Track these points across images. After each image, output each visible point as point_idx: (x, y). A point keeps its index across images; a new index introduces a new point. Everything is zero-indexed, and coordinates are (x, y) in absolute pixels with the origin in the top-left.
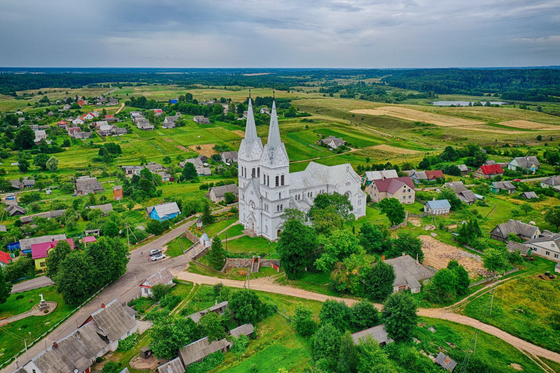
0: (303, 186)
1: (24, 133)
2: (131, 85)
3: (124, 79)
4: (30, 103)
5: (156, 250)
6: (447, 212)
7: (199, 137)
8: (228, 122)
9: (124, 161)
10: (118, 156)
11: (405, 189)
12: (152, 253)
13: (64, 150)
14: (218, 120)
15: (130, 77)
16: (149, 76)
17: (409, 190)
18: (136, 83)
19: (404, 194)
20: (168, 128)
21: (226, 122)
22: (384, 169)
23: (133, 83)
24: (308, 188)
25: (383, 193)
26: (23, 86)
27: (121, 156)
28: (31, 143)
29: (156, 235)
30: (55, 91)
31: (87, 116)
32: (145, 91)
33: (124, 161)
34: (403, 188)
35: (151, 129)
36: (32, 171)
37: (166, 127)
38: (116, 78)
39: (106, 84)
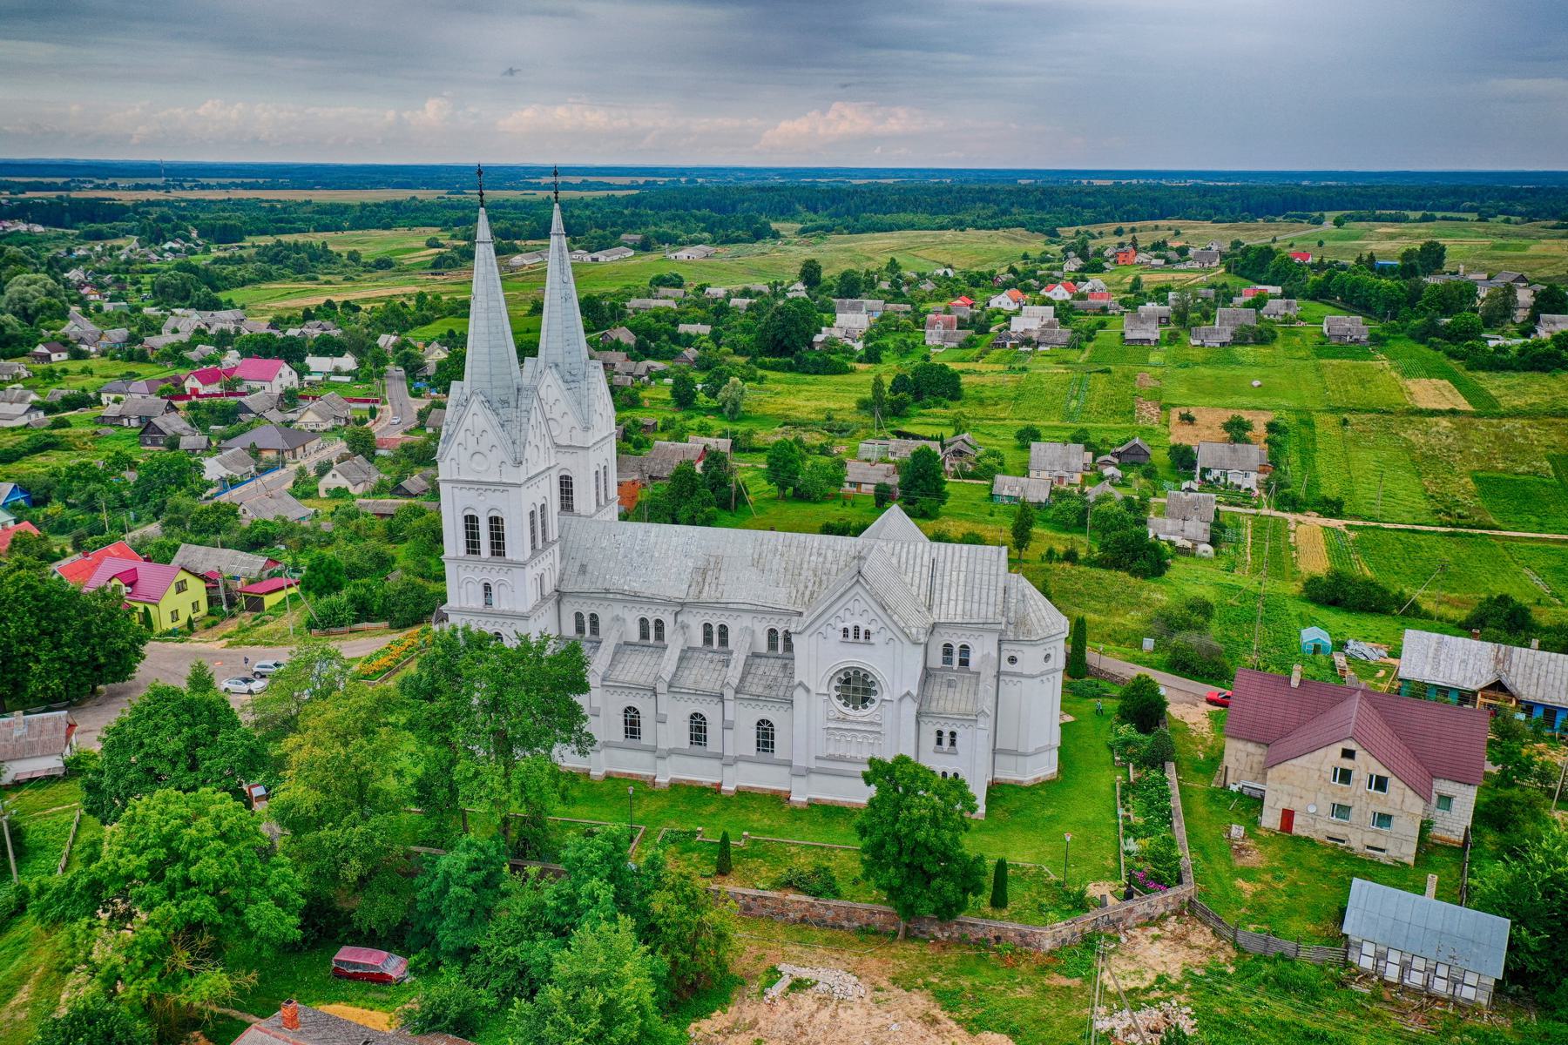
0: (679, 591)
1: (781, 314)
2: (1406, 219)
3: (1414, 202)
4: (1029, 253)
5: (271, 664)
6: (1468, 993)
7: (1256, 383)
8: (1437, 349)
9: (937, 421)
10: (938, 404)
11: (1347, 764)
12: (255, 669)
13: (853, 371)
14: (1412, 337)
15: (1421, 197)
16: (1446, 193)
17: (1381, 784)
18: (1419, 214)
19: (1343, 794)
20: (1203, 346)
21: (1433, 346)
22: (1535, 643)
23: (1412, 215)
24: (698, 605)
25: (1251, 747)
26: (1107, 214)
27: (946, 407)
28: (786, 342)
29: (391, 627)
30: (1157, 227)
31: (1055, 290)
32: (1401, 235)
33: (937, 421)
34: (1331, 756)
35: (1149, 341)
36: (699, 408)
37: (1198, 342)
38: (1390, 197)
39: (1316, 214)
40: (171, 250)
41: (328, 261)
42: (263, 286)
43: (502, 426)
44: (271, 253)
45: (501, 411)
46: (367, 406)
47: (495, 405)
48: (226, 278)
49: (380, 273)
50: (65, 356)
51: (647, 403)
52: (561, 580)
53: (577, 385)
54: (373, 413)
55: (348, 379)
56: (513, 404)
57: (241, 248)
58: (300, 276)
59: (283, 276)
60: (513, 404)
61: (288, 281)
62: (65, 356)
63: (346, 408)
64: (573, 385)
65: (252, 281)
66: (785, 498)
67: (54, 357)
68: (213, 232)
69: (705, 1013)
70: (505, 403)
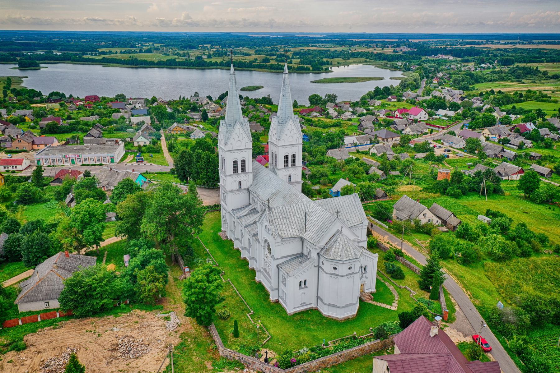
40: (481, 67)
41: (534, 75)
42: (497, 83)
43: (227, 132)
44: (512, 70)
45: (229, 128)
46: (431, 128)
47: (228, 125)
48: (484, 79)
49: (552, 80)
50: (396, 100)
51: (555, 148)
52: (251, 185)
53: (282, 125)
54: (431, 132)
55: (446, 119)
56: (232, 126)
57: (508, 67)
58: (514, 80)
59: (509, 79)
60: (232, 126)
61: (509, 81)
62: (396, 100)
63: (426, 128)
64: (281, 125)
65: (495, 80)
66: (525, 198)
67: (392, 100)
68: (502, 61)
69: (141, 310)
70: (230, 125)
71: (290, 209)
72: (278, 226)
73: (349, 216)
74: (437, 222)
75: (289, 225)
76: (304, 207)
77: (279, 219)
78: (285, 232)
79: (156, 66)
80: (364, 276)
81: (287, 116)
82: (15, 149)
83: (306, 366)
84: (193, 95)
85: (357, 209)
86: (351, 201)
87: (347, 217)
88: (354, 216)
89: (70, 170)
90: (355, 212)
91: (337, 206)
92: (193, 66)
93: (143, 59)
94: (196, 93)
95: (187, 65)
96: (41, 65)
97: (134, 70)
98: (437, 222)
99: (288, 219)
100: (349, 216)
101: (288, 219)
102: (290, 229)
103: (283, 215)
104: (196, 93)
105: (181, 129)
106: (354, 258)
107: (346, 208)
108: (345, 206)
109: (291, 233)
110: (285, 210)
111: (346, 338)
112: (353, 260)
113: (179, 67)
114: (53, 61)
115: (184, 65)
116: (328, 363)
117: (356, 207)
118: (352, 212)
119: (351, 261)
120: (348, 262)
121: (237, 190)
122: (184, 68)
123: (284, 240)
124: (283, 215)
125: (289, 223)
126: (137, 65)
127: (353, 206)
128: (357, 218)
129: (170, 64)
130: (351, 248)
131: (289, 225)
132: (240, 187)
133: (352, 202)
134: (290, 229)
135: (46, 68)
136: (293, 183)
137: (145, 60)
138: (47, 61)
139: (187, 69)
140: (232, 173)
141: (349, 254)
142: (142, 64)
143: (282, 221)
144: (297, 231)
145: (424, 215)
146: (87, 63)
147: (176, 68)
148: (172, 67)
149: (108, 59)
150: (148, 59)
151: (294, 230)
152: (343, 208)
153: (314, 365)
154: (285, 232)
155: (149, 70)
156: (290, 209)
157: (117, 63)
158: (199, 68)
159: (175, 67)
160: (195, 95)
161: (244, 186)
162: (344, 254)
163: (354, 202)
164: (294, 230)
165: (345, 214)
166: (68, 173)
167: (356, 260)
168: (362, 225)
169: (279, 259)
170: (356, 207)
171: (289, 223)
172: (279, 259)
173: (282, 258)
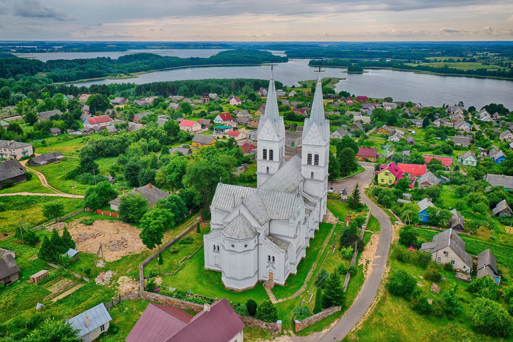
71: (236, 190)
72: (219, 199)
73: (281, 210)
74: (464, 267)
75: (228, 201)
76: (248, 191)
77: (223, 194)
78: (221, 205)
79: (464, 75)
80: (271, 265)
81: (314, 119)
82: (251, 126)
83: (156, 296)
84: (457, 104)
85: (291, 207)
86: (291, 199)
87: (278, 211)
88: (285, 212)
89: (250, 144)
90: (289, 209)
91: (276, 199)
92: (504, 76)
93: (454, 68)
94: (462, 102)
95: (497, 76)
96: (364, 70)
97: (442, 78)
98: (464, 267)
99: (229, 196)
100: (281, 210)
101: (229, 196)
102: (227, 204)
103: (228, 192)
104: (462, 102)
105: (385, 131)
106: (236, 238)
107: (282, 203)
108: (283, 201)
109: (223, 207)
110: (231, 189)
111: (208, 298)
112: (233, 240)
113: (488, 77)
114: (378, 67)
115: (495, 75)
116: (173, 303)
117: (292, 205)
118: (286, 208)
119: (231, 239)
120: (229, 239)
121: (265, 174)
122: (493, 79)
123: (216, 210)
124: (228, 192)
125: (228, 199)
126: (446, 73)
127: (290, 204)
128: (287, 214)
129: (480, 74)
130: (238, 230)
131: (228, 201)
132: (268, 172)
133: (292, 200)
134: (227, 204)
135: (367, 72)
136: (314, 180)
137: (455, 69)
138: (373, 67)
139: (497, 79)
140: (306, 163)
141: (234, 233)
142: (451, 73)
143: (225, 196)
144: (230, 207)
145: (445, 252)
146: (404, 70)
147: (485, 78)
148: (481, 76)
149: (423, 67)
150: (458, 68)
151: (229, 205)
152: (280, 202)
153: (161, 299)
154: (221, 205)
155: (457, 78)
156: (236, 190)
157: (429, 71)
158: (510, 78)
159: (484, 76)
160: (459, 105)
161: (271, 171)
162: (230, 232)
163: (293, 201)
164: (229, 205)
165: (279, 208)
166: (248, 146)
167: (236, 240)
168: (287, 221)
169: (215, 224)
170: (292, 205)
171: (228, 199)
172: (215, 224)
173: (216, 224)
